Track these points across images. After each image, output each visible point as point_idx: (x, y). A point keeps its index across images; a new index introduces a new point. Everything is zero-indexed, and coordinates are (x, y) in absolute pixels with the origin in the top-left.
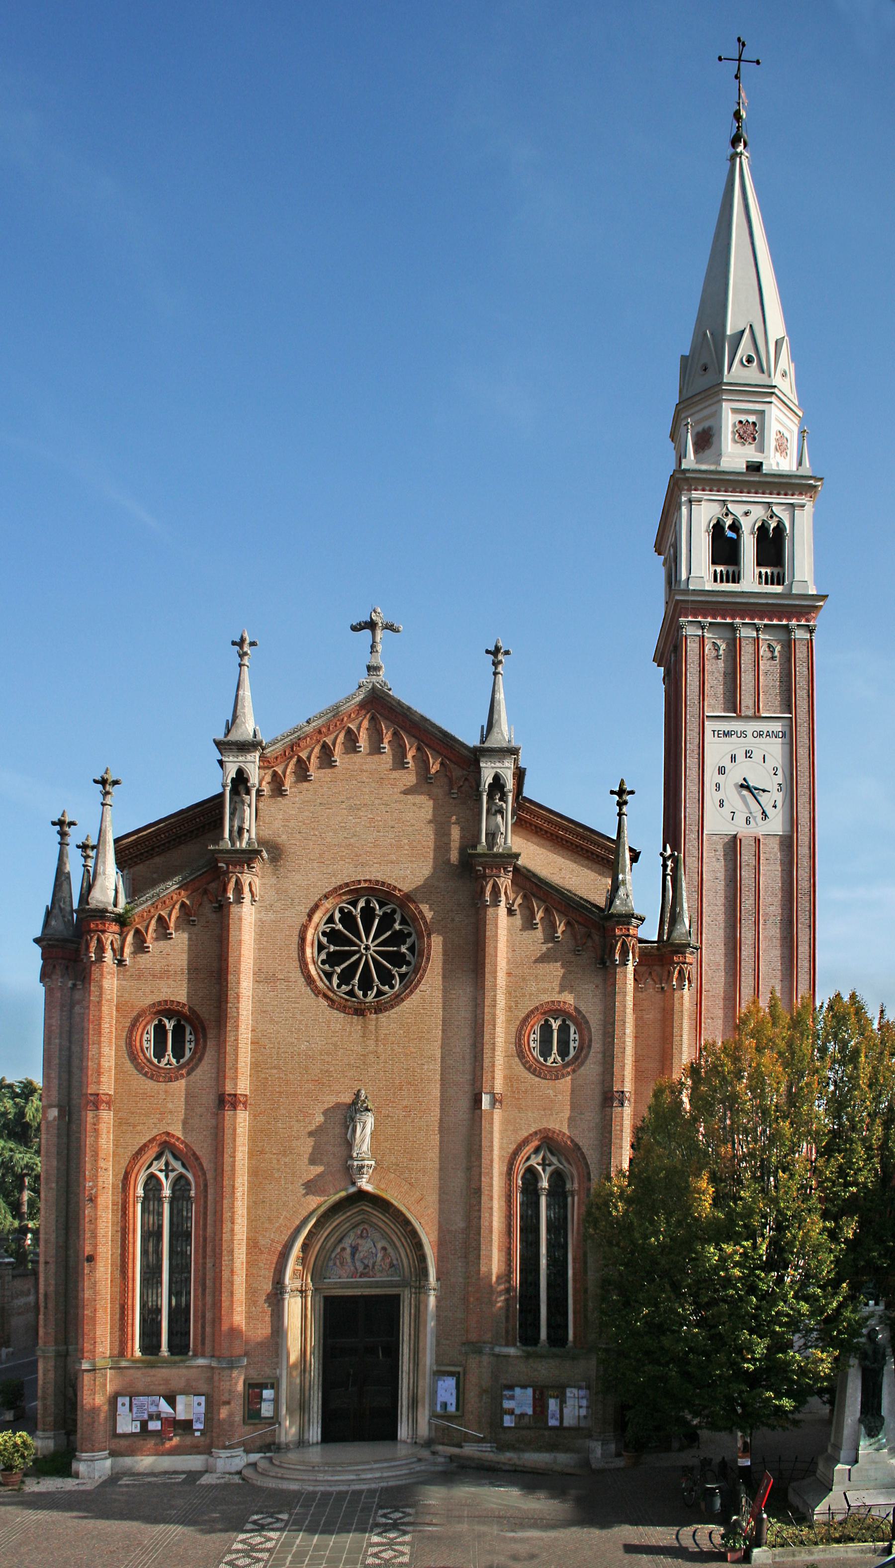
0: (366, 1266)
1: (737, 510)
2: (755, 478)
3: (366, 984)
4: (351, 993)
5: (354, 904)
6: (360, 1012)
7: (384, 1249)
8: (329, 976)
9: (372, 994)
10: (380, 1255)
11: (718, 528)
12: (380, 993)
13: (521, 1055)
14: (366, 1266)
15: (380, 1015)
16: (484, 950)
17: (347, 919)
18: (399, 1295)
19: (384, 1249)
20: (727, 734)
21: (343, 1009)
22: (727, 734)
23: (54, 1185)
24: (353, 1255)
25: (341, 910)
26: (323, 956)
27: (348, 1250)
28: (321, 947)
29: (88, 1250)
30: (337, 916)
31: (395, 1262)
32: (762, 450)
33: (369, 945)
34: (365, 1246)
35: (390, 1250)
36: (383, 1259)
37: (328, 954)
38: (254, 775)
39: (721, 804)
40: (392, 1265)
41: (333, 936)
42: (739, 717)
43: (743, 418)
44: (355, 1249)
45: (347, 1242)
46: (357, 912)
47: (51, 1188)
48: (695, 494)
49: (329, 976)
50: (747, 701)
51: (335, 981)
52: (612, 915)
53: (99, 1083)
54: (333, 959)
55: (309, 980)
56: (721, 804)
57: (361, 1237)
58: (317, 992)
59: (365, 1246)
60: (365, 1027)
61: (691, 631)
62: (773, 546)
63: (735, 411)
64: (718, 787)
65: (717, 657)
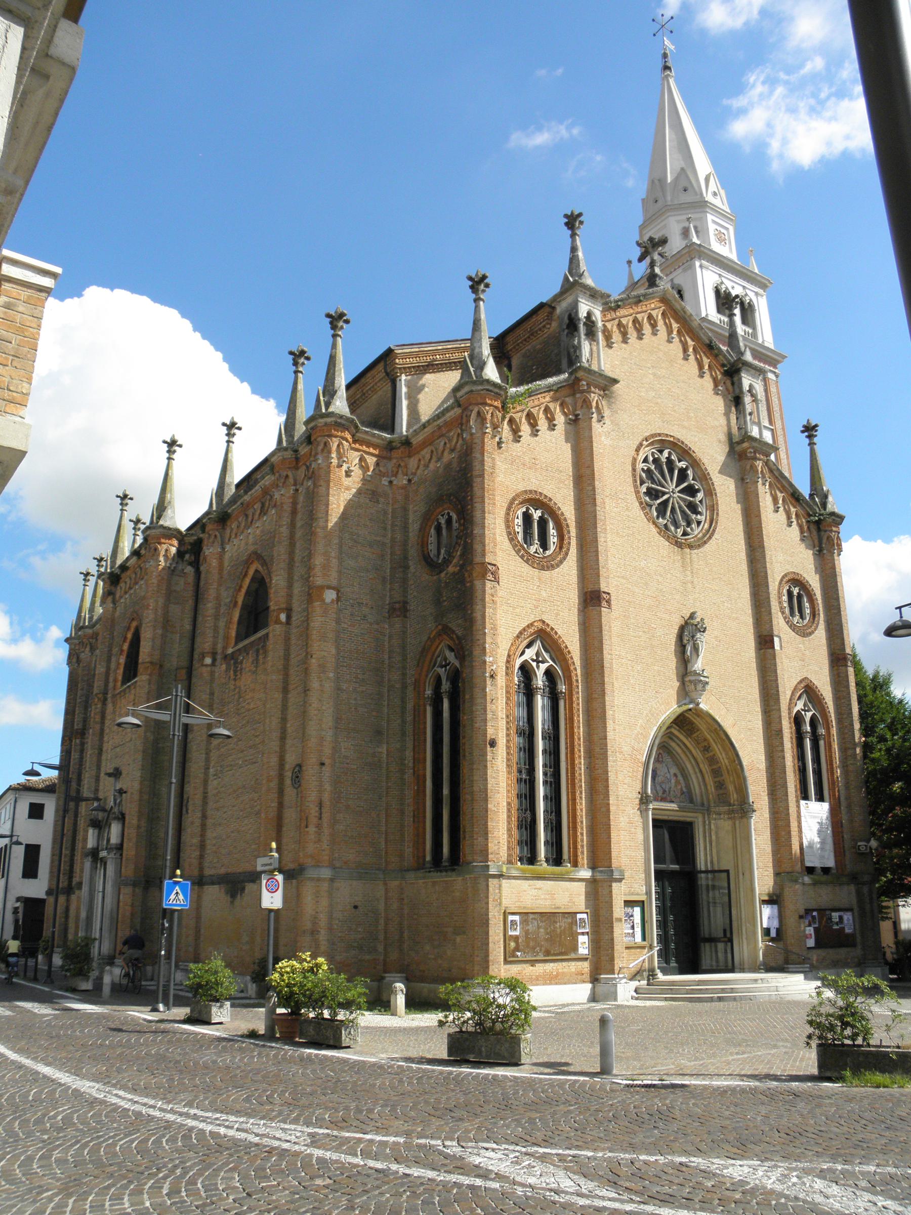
7: (675, 775)
10: (673, 781)
14: (664, 792)
15: (693, 552)
19: (675, 775)
31: (684, 790)
33: (672, 489)
36: (676, 786)
37: (648, 489)
40: (683, 793)
43: (719, 228)
53: (495, 553)
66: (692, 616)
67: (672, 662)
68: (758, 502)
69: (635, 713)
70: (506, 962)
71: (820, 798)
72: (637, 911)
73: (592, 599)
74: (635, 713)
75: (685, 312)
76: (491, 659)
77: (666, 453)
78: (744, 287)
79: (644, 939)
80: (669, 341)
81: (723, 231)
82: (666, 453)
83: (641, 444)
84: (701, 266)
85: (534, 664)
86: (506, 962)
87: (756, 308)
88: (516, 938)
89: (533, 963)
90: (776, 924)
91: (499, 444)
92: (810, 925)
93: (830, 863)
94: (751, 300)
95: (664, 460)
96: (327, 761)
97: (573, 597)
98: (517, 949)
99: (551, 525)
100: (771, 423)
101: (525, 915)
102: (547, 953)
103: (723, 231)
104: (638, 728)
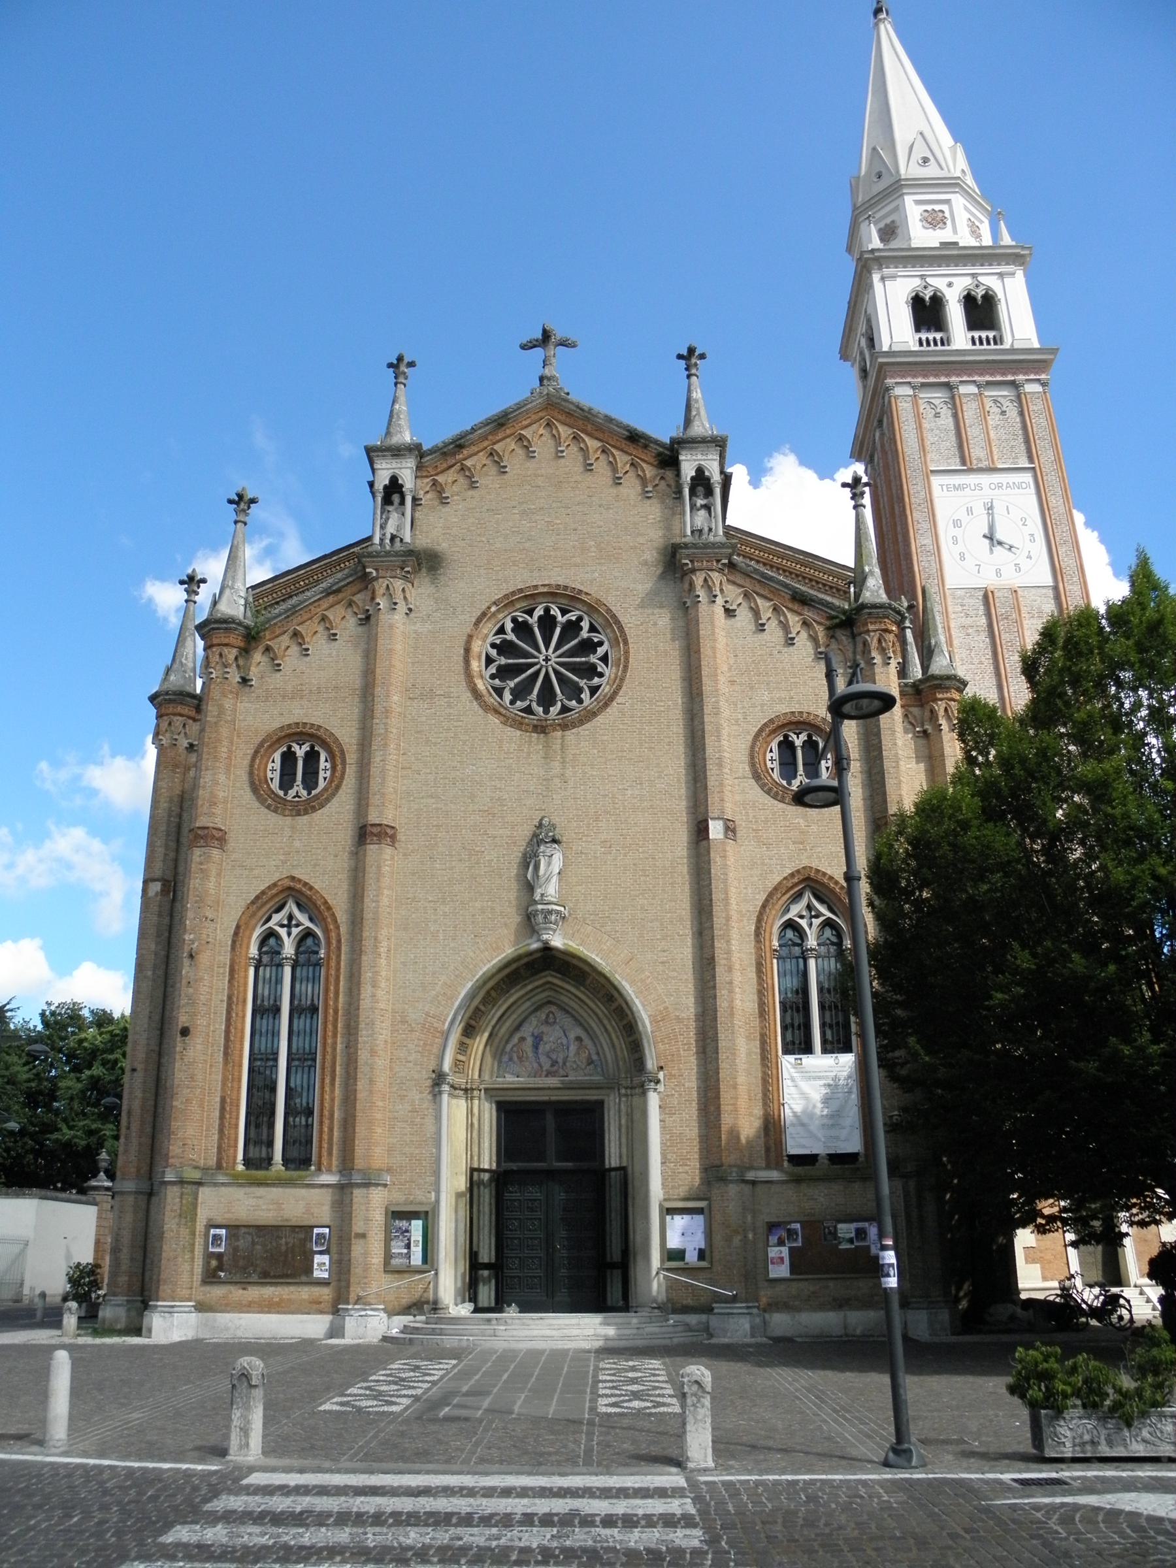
0: (554, 1063)
1: (939, 283)
2: (950, 256)
3: (547, 698)
4: (528, 710)
5: (530, 612)
6: (541, 729)
7: (579, 1039)
8: (499, 692)
9: (554, 710)
10: (573, 1048)
11: (917, 302)
12: (565, 709)
13: (757, 776)
14: (554, 1063)
15: (567, 733)
16: (698, 651)
17: (522, 628)
18: (601, 1103)
19: (579, 1039)
20: (957, 488)
21: (518, 724)
22: (957, 488)
23: (150, 973)
24: (536, 1047)
25: (514, 620)
26: (493, 669)
27: (530, 1040)
28: (489, 661)
29: (183, 1020)
30: (509, 626)
31: (595, 1057)
32: (955, 231)
33: (548, 657)
34: (553, 1036)
35: (587, 1041)
36: (577, 1053)
38: (408, 479)
40: (590, 1062)
41: (504, 648)
43: (929, 208)
44: (538, 1039)
45: (527, 1030)
46: (533, 620)
47: (145, 977)
49: (499, 692)
50: (977, 452)
51: (508, 696)
52: (863, 606)
54: (504, 673)
55: (476, 694)
57: (547, 1022)
58: (486, 707)
59: (553, 1036)
60: (547, 746)
61: (899, 391)
62: (981, 310)
65: (937, 415)
66: (540, 826)
67: (510, 894)
68: (698, 631)
69: (421, 968)
70: (205, 1282)
72: (417, 1226)
73: (367, 834)
74: (421, 968)
75: (582, 410)
76: (192, 936)
78: (974, 276)
79: (425, 1259)
80: (558, 455)
81: (937, 207)
83: (484, 614)
84: (883, 279)
86: (205, 1282)
87: (1000, 295)
88: (219, 1256)
89: (244, 1284)
90: (699, 1241)
91: (245, 681)
92: (781, 1243)
93: (853, 1144)
94: (988, 289)
95: (533, 620)
96: (140, 1067)
97: (345, 836)
98: (220, 1268)
99: (323, 756)
100: (1031, 460)
101: (234, 1229)
102: (265, 1274)
103: (937, 207)
104: (438, 988)
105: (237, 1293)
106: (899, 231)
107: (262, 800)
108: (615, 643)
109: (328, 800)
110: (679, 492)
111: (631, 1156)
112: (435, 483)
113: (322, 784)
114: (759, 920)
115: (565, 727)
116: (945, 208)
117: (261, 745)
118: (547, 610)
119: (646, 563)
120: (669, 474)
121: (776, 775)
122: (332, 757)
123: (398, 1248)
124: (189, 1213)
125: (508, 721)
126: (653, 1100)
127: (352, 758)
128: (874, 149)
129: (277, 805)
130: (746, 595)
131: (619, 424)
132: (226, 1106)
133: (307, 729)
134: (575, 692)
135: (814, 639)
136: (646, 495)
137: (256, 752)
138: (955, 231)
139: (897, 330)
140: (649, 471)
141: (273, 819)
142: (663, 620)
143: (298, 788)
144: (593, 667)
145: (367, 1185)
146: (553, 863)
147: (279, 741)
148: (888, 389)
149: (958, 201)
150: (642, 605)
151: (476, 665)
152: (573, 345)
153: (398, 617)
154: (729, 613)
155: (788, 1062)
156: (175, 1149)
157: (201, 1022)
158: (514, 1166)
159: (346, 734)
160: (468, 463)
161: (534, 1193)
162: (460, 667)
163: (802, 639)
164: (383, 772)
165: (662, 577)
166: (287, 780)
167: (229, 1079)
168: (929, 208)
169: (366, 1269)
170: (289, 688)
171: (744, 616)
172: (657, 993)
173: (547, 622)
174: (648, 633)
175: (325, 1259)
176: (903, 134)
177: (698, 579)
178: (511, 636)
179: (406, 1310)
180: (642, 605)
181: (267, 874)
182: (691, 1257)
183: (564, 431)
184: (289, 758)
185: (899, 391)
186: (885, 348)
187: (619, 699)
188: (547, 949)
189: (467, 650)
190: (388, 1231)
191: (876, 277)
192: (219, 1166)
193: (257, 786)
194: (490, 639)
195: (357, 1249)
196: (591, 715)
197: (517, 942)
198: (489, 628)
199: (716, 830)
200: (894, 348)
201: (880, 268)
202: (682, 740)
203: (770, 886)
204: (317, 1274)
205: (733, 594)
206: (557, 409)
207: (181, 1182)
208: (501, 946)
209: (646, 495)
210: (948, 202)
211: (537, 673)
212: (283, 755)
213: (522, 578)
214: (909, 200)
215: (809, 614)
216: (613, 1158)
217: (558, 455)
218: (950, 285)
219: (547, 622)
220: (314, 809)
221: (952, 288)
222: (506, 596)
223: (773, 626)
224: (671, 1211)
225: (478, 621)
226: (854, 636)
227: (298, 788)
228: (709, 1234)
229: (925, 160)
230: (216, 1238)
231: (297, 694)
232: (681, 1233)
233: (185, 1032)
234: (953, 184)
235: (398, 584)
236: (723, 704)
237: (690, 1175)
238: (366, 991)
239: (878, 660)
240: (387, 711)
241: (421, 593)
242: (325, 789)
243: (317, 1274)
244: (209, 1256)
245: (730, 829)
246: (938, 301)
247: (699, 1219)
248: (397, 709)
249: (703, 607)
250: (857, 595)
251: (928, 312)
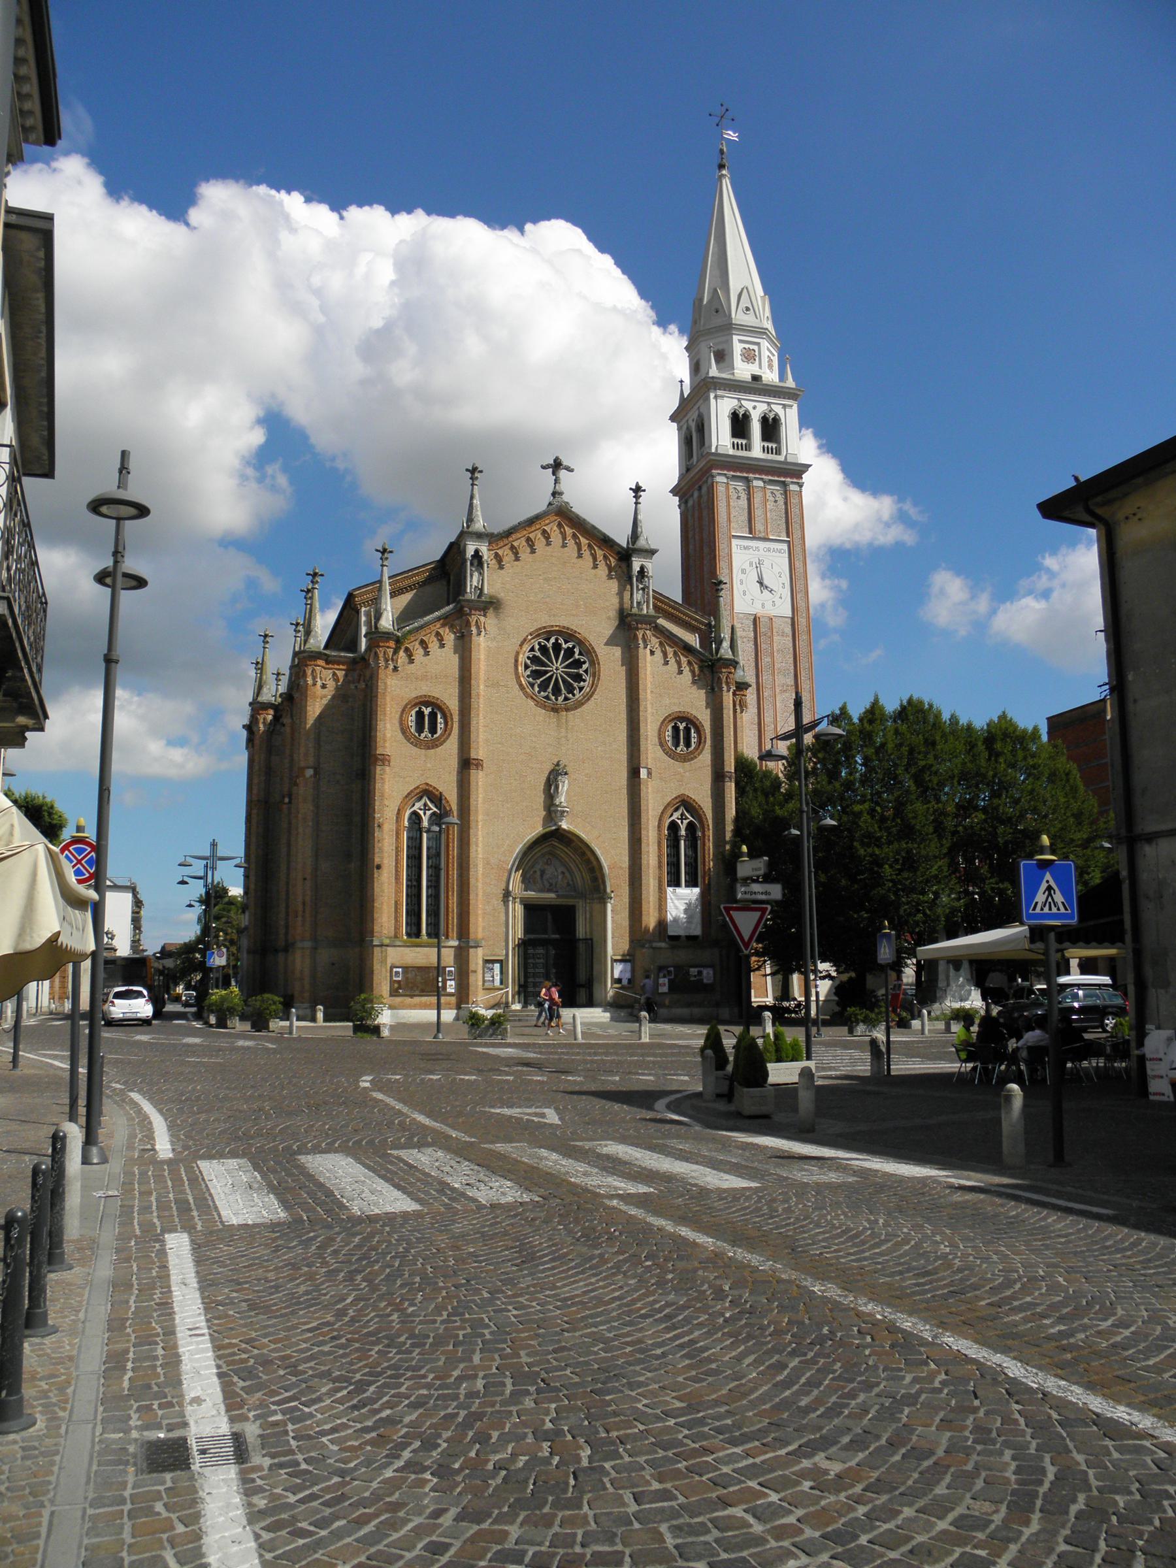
0: (551, 885)
1: (748, 405)
2: (755, 386)
4: (547, 697)
5: (548, 640)
6: (555, 710)
8: (532, 685)
9: (561, 699)
11: (735, 417)
12: (566, 699)
13: (661, 745)
14: (551, 885)
16: (637, 675)
17: (543, 649)
21: (544, 707)
24: (542, 876)
25: (539, 644)
26: (528, 672)
27: (538, 873)
28: (527, 667)
30: (537, 647)
32: (760, 367)
33: (557, 668)
34: (550, 871)
35: (567, 874)
37: (532, 671)
39: (744, 594)
40: (568, 885)
41: (534, 660)
42: (754, 538)
43: (747, 346)
44: (543, 872)
45: (538, 867)
46: (549, 645)
48: (719, 393)
49: (532, 685)
51: (537, 689)
54: (536, 674)
55: (521, 685)
56: (744, 594)
57: (547, 863)
58: (527, 695)
59: (550, 871)
60: (558, 720)
61: (719, 479)
63: (741, 341)
64: (742, 583)
65: (738, 498)
66: (558, 765)
67: (540, 798)
69: (498, 839)
70: (391, 995)
71: (692, 883)
72: (497, 966)
73: (466, 764)
74: (498, 839)
77: (553, 640)
78: (769, 404)
79: (501, 983)
80: (564, 546)
81: (752, 347)
82: (553, 640)
83: (525, 640)
84: (716, 397)
85: (421, 813)
86: (391, 995)
87: (783, 421)
88: (399, 982)
89: (412, 996)
90: (628, 975)
91: (395, 669)
92: (664, 976)
93: (697, 931)
94: (776, 415)
95: (549, 645)
96: (308, 877)
97: (454, 763)
98: (400, 988)
101: (406, 969)
102: (423, 991)
103: (752, 347)
105: (408, 1000)
106: (727, 357)
107: (406, 737)
108: (592, 663)
109: (444, 741)
110: (630, 578)
111: (591, 933)
112: (496, 554)
113: (439, 732)
114: (660, 820)
115: (567, 710)
116: (755, 348)
117: (406, 706)
118: (557, 640)
119: (609, 618)
120: (624, 565)
121: (670, 744)
122: (445, 717)
123: (488, 977)
124: (384, 961)
125: (538, 704)
126: (609, 907)
127: (456, 718)
128: (715, 290)
129: (417, 743)
130: (661, 644)
131: (599, 531)
132: (397, 905)
133: (431, 699)
134: (571, 690)
135: (693, 672)
136: (610, 577)
137: (403, 710)
138: (760, 367)
139: (721, 438)
140: (613, 562)
141: (415, 751)
142: (617, 652)
143: (426, 732)
144: (581, 675)
145: (476, 947)
146: (564, 786)
147: (415, 705)
148: (713, 477)
149: (765, 344)
150: (607, 644)
151: (521, 669)
152: (572, 471)
153: (482, 638)
154: (652, 653)
155: (670, 890)
156: (376, 928)
157: (386, 861)
158: (532, 936)
159: (452, 703)
160: (515, 544)
161: (540, 951)
162: (512, 670)
163: (686, 670)
164: (478, 730)
165: (618, 627)
166: (420, 729)
167: (398, 892)
168: (747, 346)
169: (477, 987)
170: (419, 673)
171: (659, 654)
172: (612, 855)
173: (557, 647)
174: (610, 659)
175: (453, 983)
176: (735, 285)
177: (640, 634)
178: (538, 654)
179: (492, 1008)
180: (607, 644)
181: (414, 781)
182: (625, 982)
183: (569, 531)
184: (420, 715)
185: (719, 479)
186: (713, 450)
187: (595, 696)
188: (559, 829)
189: (516, 661)
190: (484, 968)
191: (712, 395)
192: (396, 937)
193: (404, 730)
194: (527, 654)
195: (472, 978)
196: (580, 704)
197: (544, 826)
198: (526, 647)
199: (643, 773)
200: (720, 451)
201: (715, 389)
202: (625, 722)
203: (666, 803)
204: (449, 990)
205: (654, 642)
206: (565, 515)
207: (381, 946)
208: (536, 829)
209: (610, 577)
210: (758, 344)
211: (551, 677)
212: (417, 713)
213: (545, 620)
214: (735, 338)
215: (691, 658)
216: (581, 932)
217: (564, 546)
218: (754, 408)
219: (557, 647)
220: (437, 746)
221: (756, 408)
222: (537, 630)
223: (672, 661)
224: (616, 961)
225: (521, 645)
226: (713, 672)
227: (426, 732)
228: (633, 971)
229: (748, 309)
230: (397, 973)
231: (424, 678)
232: (618, 970)
233: (379, 867)
234: (761, 332)
235: (482, 619)
236: (649, 706)
237: (625, 946)
238: (473, 848)
239: (725, 688)
240: (478, 695)
241: (489, 621)
242: (442, 735)
243: (449, 990)
244: (392, 982)
245: (649, 773)
246: (747, 416)
247: (629, 965)
248: (482, 693)
249: (641, 650)
250: (718, 650)
251: (740, 425)
